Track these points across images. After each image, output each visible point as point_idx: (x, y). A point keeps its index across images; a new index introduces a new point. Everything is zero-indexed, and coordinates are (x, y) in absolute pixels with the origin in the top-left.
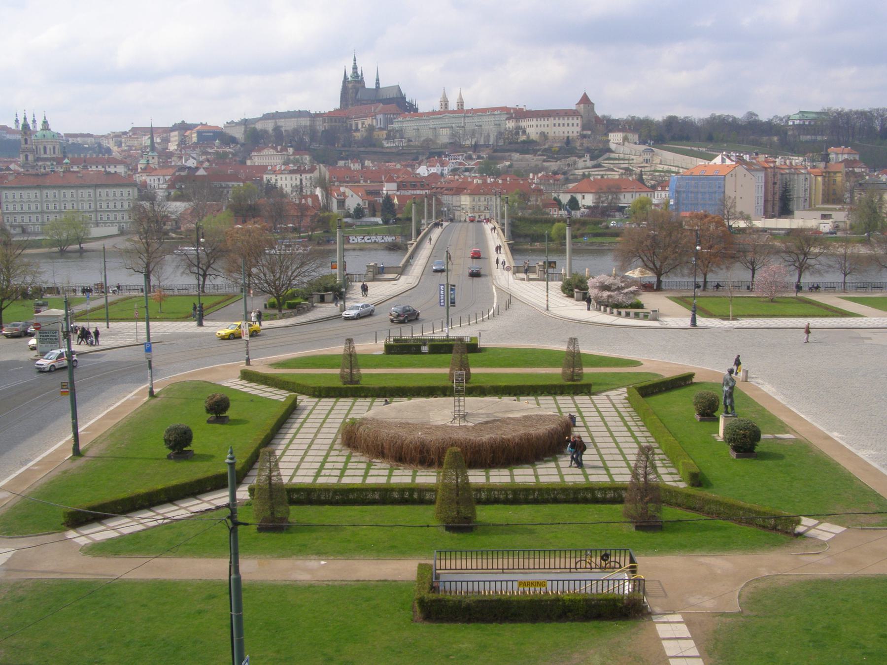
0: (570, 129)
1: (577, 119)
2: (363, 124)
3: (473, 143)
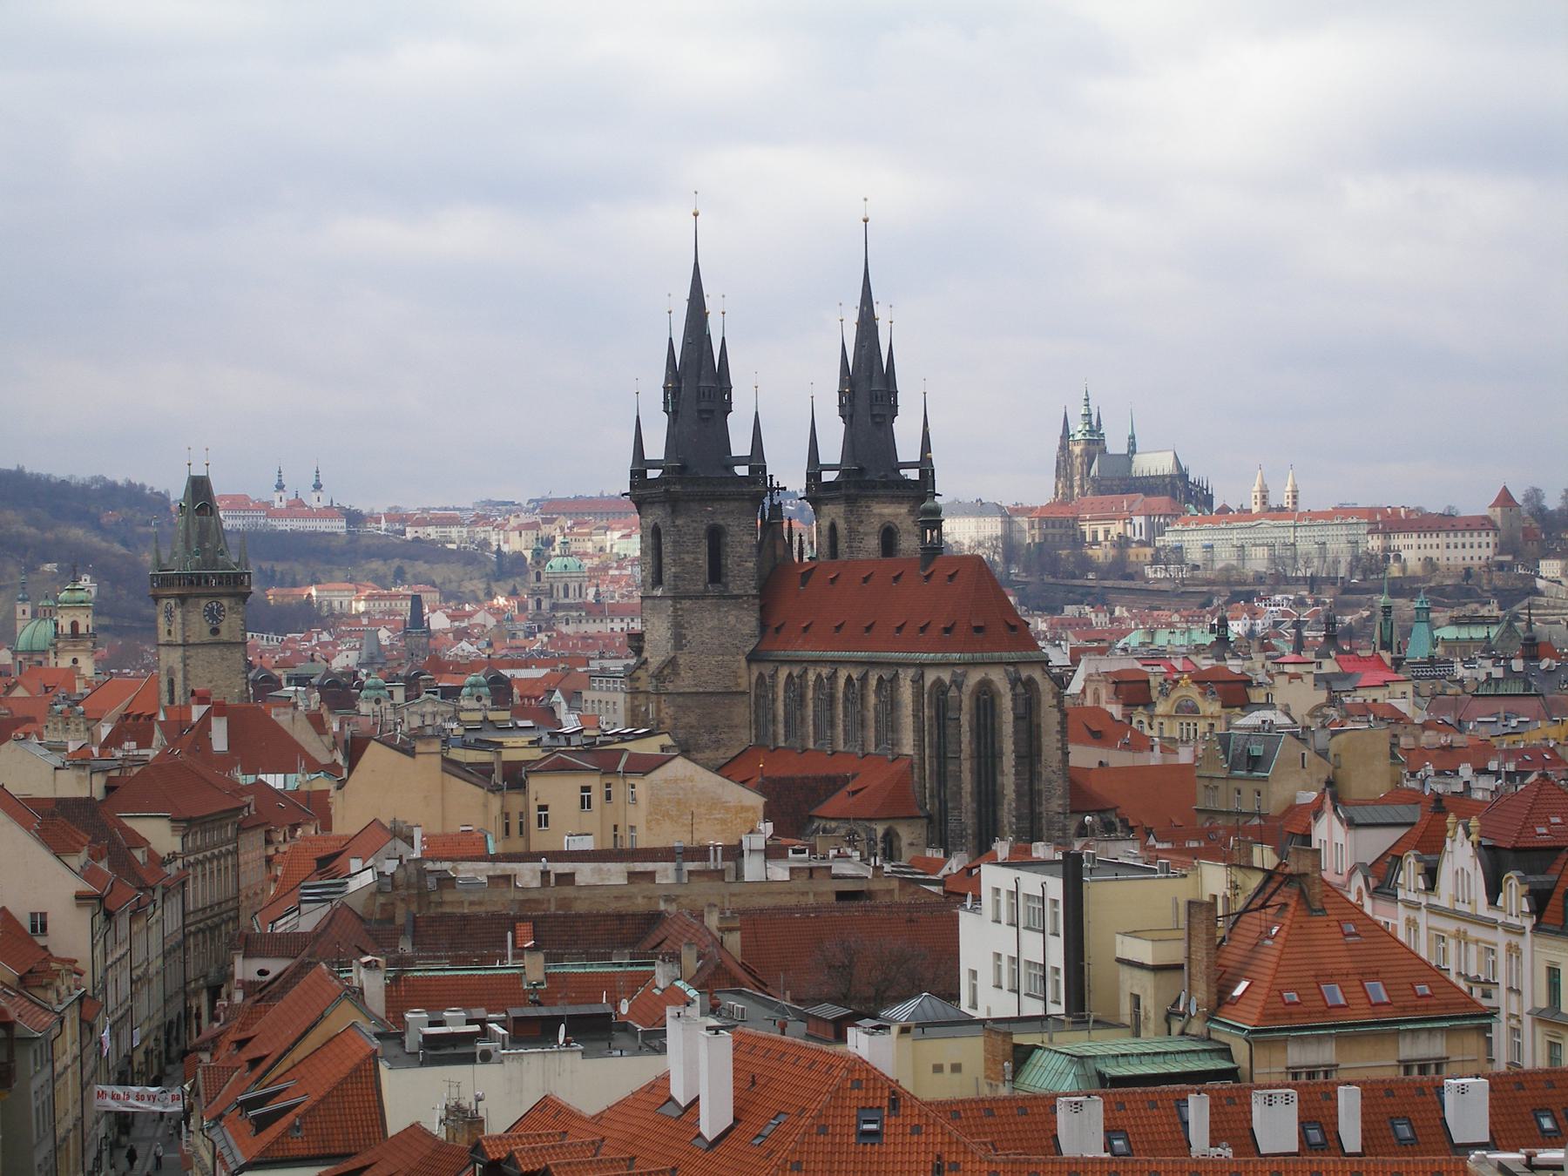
0: (1476, 552)
1: (1488, 535)
2: (1107, 532)
3: (1308, 575)
